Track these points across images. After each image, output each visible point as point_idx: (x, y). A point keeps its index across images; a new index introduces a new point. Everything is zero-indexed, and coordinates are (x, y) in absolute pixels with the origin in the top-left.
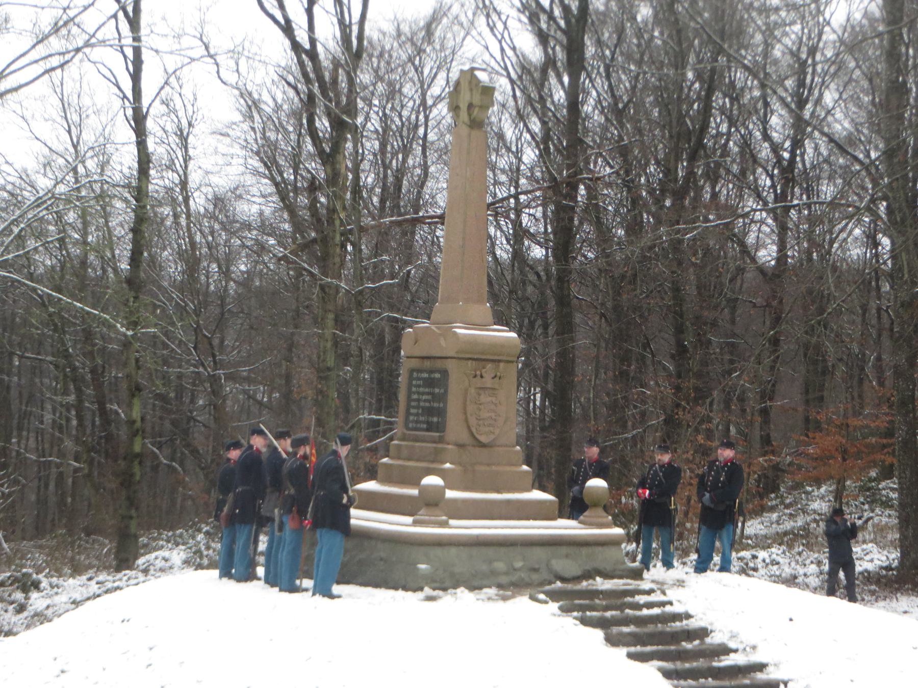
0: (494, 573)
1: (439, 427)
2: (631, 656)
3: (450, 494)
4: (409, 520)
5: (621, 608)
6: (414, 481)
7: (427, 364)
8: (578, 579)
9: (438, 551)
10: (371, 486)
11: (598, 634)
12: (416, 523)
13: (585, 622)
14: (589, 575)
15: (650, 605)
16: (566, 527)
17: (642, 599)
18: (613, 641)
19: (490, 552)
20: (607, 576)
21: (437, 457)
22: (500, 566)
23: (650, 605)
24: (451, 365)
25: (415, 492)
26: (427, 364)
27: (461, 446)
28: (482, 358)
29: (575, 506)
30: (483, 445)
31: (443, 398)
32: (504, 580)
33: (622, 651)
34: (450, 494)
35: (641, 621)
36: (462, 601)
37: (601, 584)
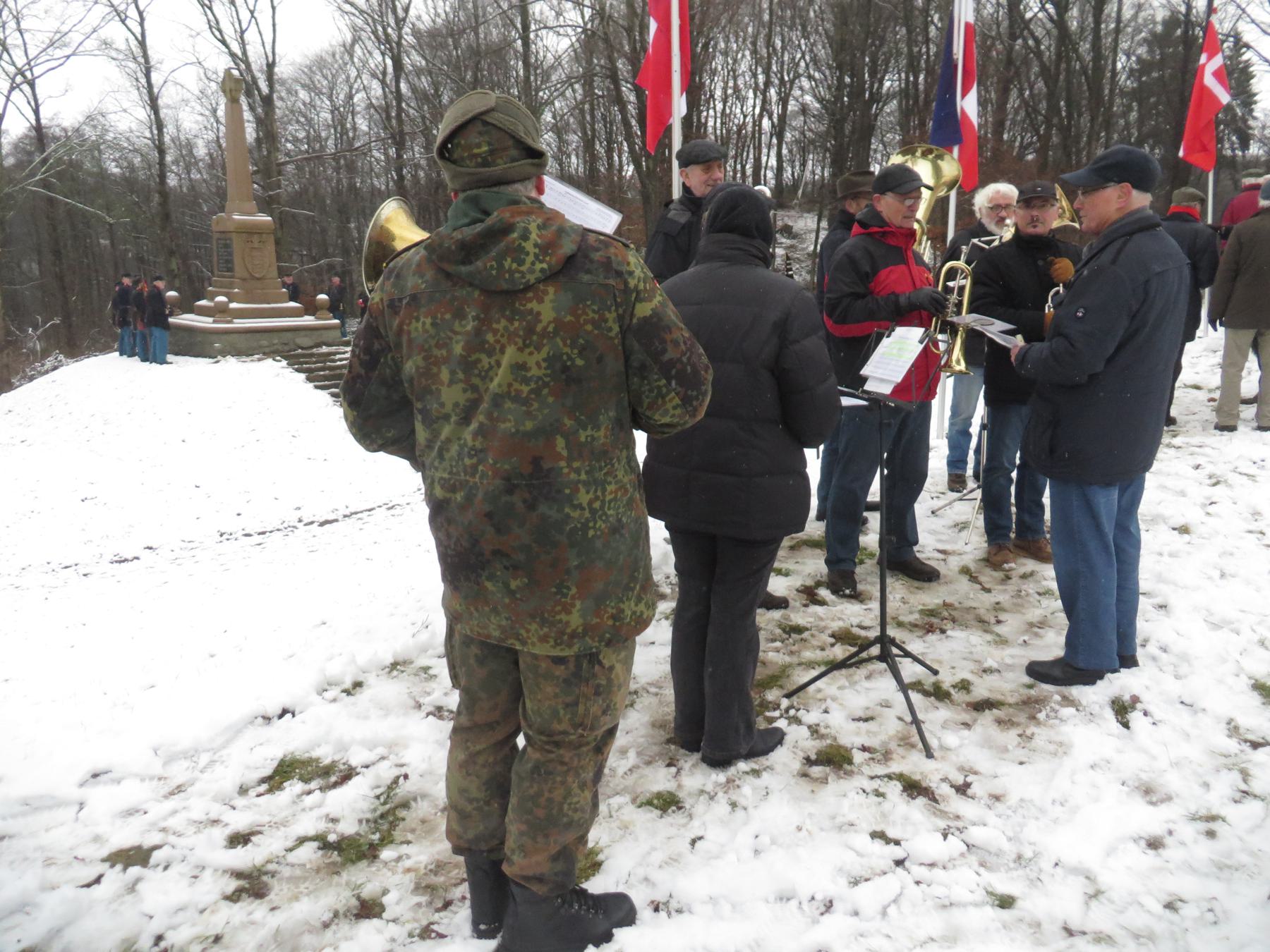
0: (261, 347)
1: (230, 270)
2: (317, 387)
3: (233, 305)
4: (211, 320)
5: (324, 362)
6: (212, 299)
7: (223, 236)
8: (312, 347)
9: (225, 337)
10: (203, 302)
11: (303, 376)
12: (214, 322)
13: (298, 370)
14: (319, 345)
15: (341, 360)
16: (308, 320)
17: (338, 357)
18: (309, 379)
19: (258, 335)
20: (328, 345)
21: (231, 286)
22: (265, 343)
23: (341, 360)
24: (234, 236)
25: (212, 304)
26: (223, 236)
27: (244, 280)
28: (250, 231)
29: (311, 309)
30: (253, 278)
31: (231, 254)
32: (267, 350)
33: (311, 385)
34: (233, 305)
35: (331, 368)
36: (230, 364)
37: (325, 349)
